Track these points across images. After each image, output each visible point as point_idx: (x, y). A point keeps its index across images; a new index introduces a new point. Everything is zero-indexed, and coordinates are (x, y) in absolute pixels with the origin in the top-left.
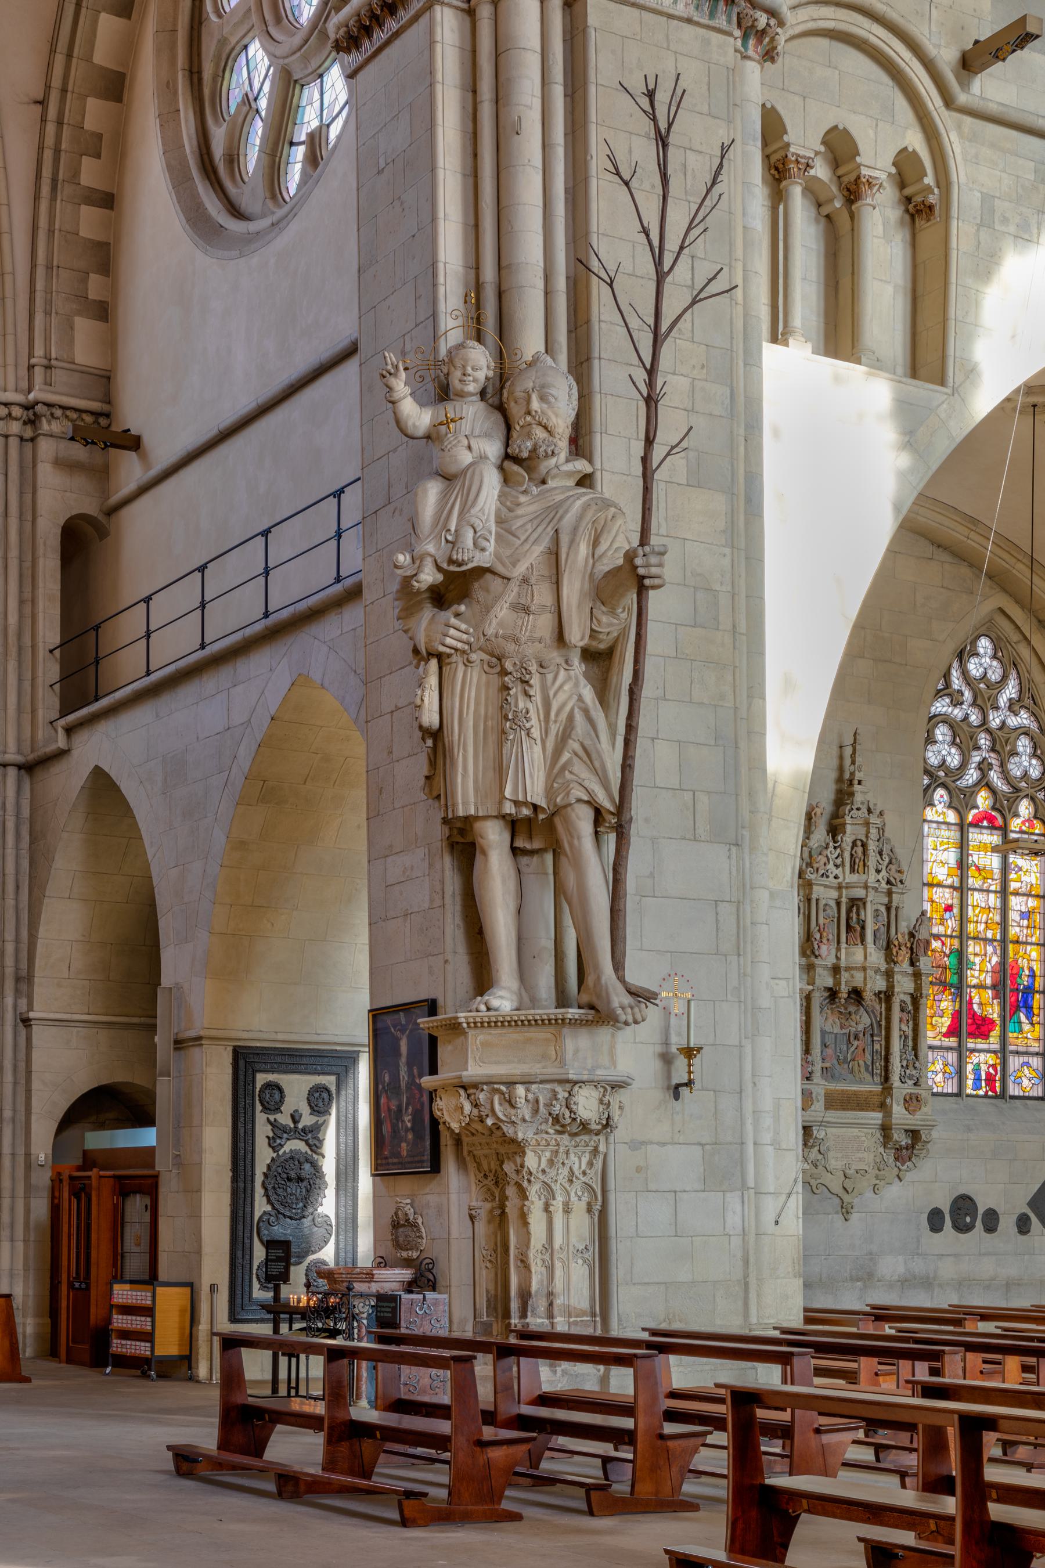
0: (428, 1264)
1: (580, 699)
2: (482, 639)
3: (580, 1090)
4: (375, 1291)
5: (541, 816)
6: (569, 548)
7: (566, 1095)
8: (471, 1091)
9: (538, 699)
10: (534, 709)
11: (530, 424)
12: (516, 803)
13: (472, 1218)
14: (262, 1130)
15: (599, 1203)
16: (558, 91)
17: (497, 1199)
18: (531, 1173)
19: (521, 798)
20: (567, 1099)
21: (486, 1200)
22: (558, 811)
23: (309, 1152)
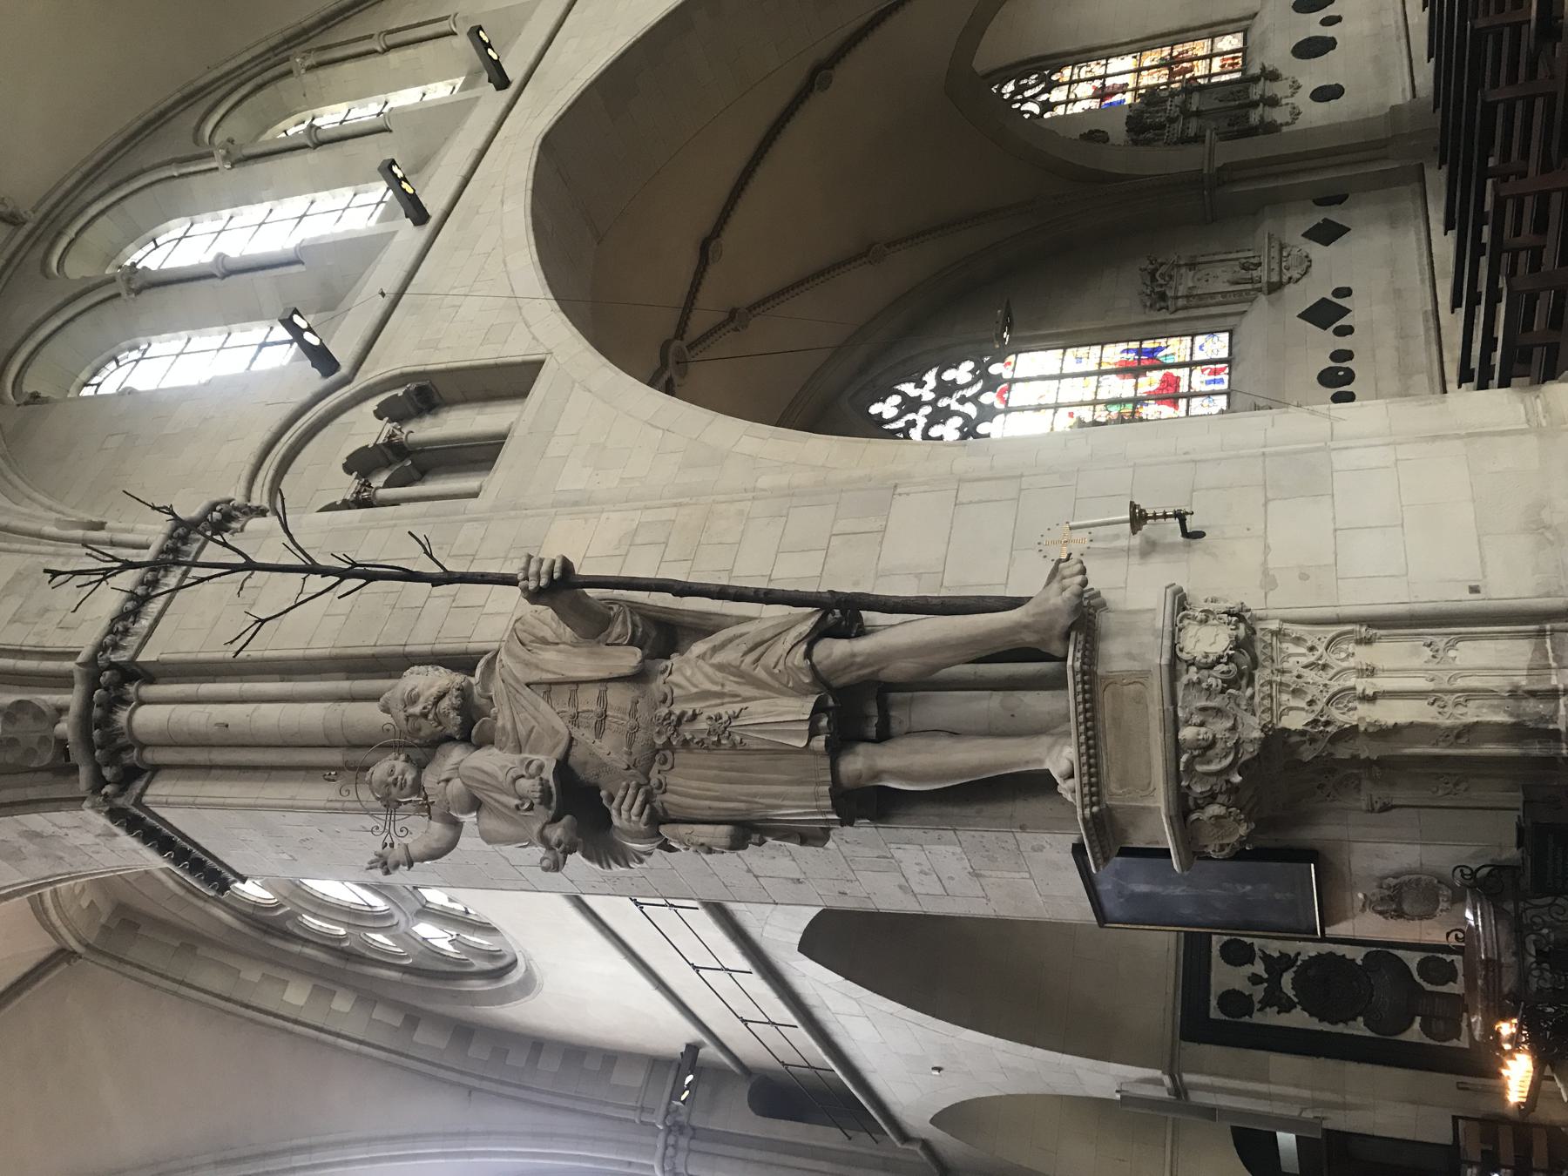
0: (1463, 875)
1: (702, 657)
2: (633, 771)
3: (1186, 650)
4: (1514, 959)
5: (831, 702)
6: (542, 670)
7: (1193, 669)
8: (1191, 803)
9: (697, 706)
10: (708, 709)
11: (436, 714)
12: (813, 733)
13: (1386, 808)
14: (1272, 1017)
15: (1356, 627)
16: (207, 688)
17: (1355, 771)
18: (1315, 722)
19: (806, 727)
20: (1200, 669)
21: (1358, 788)
22: (820, 679)
23: (1294, 969)
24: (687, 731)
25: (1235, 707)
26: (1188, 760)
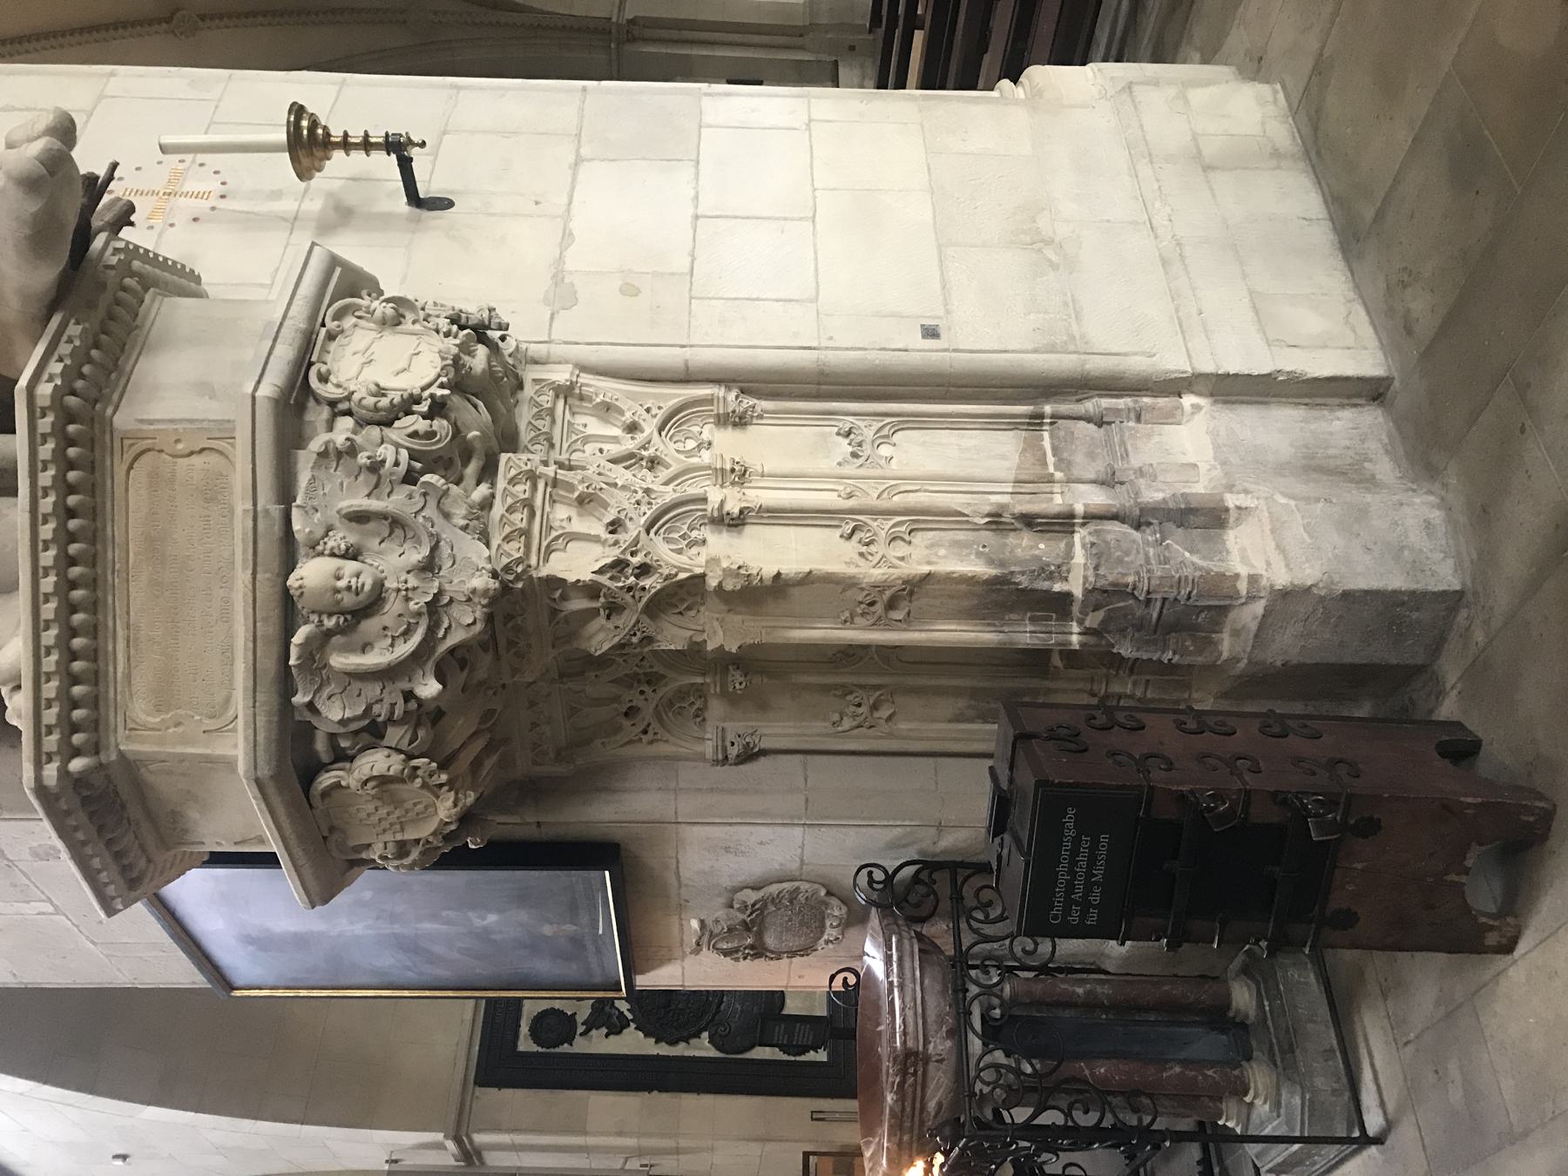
0: (871, 881)
4: (949, 1043)
7: (346, 423)
8: (321, 745)
13: (749, 755)
15: (719, 391)
17: (699, 680)
18: (619, 565)
20: (362, 423)
21: (700, 715)
25: (439, 520)
26: (309, 640)
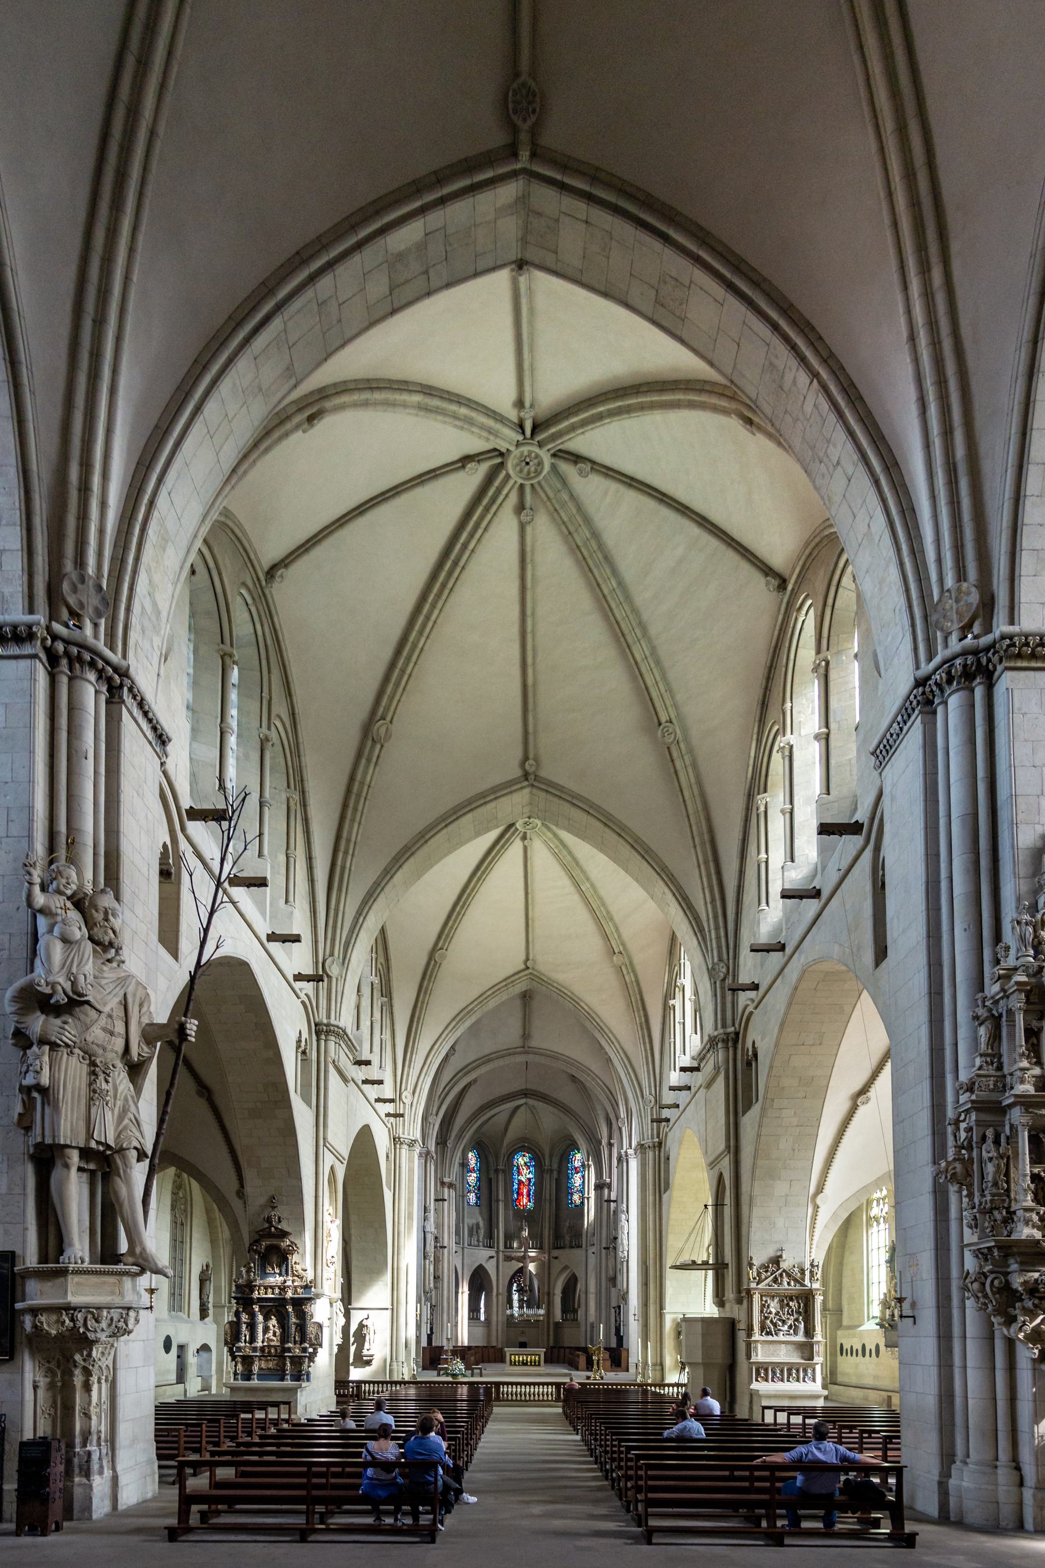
12: (98, 1143)
19: (103, 1141)
22: (121, 1150)
24: (102, 1077)
